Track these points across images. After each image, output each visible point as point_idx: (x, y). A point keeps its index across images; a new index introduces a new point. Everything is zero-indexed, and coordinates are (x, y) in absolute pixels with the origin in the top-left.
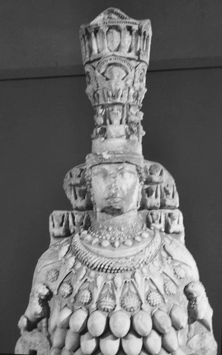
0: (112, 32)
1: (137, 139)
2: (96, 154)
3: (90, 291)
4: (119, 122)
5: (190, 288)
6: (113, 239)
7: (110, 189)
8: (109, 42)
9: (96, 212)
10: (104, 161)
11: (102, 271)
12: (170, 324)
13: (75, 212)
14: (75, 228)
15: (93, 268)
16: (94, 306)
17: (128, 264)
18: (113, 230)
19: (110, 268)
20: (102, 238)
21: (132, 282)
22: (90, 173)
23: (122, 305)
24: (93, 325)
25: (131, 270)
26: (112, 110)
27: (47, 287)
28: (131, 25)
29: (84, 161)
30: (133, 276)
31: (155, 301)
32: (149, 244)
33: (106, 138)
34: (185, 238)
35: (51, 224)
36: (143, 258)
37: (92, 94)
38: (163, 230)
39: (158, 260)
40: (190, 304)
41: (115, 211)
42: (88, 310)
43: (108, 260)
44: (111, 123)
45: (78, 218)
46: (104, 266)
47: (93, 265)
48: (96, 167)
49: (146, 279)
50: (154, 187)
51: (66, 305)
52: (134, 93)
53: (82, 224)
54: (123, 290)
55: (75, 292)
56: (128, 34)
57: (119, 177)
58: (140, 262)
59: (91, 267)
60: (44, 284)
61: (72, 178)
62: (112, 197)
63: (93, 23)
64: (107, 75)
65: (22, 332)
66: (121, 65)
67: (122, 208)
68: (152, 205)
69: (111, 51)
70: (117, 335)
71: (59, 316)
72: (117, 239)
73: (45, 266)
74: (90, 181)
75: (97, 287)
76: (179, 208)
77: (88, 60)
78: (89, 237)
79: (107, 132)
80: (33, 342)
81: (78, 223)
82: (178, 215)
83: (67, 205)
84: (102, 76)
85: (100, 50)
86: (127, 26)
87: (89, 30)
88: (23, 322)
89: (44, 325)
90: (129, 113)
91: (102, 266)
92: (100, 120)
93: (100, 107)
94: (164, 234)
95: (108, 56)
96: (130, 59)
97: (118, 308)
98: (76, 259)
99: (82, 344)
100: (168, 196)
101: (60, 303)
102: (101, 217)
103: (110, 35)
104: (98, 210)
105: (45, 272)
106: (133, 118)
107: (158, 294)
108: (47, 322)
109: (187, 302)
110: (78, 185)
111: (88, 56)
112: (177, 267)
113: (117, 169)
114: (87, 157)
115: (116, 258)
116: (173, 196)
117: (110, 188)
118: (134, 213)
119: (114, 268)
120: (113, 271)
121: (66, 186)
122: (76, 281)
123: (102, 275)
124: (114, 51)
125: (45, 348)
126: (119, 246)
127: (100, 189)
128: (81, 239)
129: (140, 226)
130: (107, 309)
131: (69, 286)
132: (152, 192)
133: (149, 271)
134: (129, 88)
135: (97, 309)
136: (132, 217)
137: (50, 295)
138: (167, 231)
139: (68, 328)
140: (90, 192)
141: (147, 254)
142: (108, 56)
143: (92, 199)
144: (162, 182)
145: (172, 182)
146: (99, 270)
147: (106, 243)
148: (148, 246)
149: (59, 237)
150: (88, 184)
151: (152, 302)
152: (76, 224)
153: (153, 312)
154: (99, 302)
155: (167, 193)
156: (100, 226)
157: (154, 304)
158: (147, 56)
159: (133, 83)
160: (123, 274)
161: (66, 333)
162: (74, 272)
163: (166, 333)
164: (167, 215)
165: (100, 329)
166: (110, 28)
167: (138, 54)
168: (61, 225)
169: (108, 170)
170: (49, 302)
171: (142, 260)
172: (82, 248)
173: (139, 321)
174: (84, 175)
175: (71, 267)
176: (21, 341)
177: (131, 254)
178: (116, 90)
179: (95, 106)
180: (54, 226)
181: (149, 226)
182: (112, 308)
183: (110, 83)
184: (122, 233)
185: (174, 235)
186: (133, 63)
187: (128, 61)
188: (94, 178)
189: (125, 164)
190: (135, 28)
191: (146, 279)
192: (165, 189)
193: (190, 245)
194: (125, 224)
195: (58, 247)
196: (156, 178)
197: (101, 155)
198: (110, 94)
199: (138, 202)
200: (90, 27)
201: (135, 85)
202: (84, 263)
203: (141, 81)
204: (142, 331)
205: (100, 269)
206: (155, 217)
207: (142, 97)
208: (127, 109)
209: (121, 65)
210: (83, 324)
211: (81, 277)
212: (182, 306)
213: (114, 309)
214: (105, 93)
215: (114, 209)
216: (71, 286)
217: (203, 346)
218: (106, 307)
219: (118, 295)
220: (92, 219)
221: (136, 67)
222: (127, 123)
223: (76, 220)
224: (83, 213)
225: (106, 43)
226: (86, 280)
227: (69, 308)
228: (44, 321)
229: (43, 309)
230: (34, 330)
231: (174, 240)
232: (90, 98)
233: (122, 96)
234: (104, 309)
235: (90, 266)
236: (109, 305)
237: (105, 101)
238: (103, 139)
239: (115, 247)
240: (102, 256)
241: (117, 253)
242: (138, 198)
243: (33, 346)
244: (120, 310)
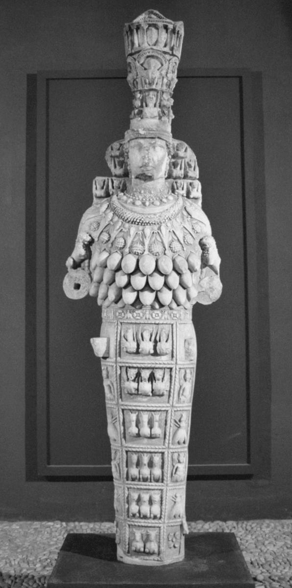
0: (151, 29)
1: (167, 120)
2: (133, 130)
3: (124, 239)
4: (153, 106)
5: (204, 241)
6: (144, 199)
7: (143, 159)
8: (148, 37)
9: (131, 178)
10: (140, 136)
11: (135, 224)
12: (187, 268)
13: (114, 178)
14: (114, 191)
15: (127, 221)
16: (127, 250)
17: (156, 219)
18: (145, 193)
19: (141, 222)
20: (135, 199)
21: (158, 232)
22: (128, 146)
23: (150, 251)
24: (126, 265)
25: (158, 224)
26: (148, 95)
27: (90, 236)
28: (167, 24)
29: (123, 137)
30: (159, 229)
31: (176, 248)
32: (173, 205)
33: (142, 118)
34: (203, 203)
35: (94, 187)
36: (168, 215)
37: (132, 81)
38: (185, 195)
39: (180, 218)
40: (203, 253)
41: (147, 178)
42: (122, 253)
43: (140, 215)
44: (147, 106)
45: (116, 183)
46: (137, 219)
47: (127, 219)
48: (133, 141)
49: (170, 231)
50: (179, 161)
51: (105, 249)
52: (168, 82)
53: (119, 188)
54: (151, 239)
55: (112, 239)
56: (164, 31)
57: (151, 150)
58: (166, 218)
59: (126, 220)
60: (87, 233)
61: (113, 150)
62: (145, 166)
63: (135, 21)
64: (146, 66)
65: (69, 269)
66: (157, 58)
67: (153, 175)
68: (178, 176)
69: (149, 45)
70: (145, 274)
71: (98, 257)
72: (148, 199)
73: (88, 219)
74: (127, 153)
75: (130, 235)
76: (199, 179)
77: (130, 52)
78: (125, 198)
79: (143, 113)
80: (78, 277)
81: (116, 187)
82: (198, 185)
83: (107, 173)
84: (141, 66)
85: (140, 44)
86: (164, 25)
87: (132, 26)
88: (70, 262)
90: (162, 98)
91: (135, 220)
92: (137, 103)
93: (138, 92)
94: (186, 198)
95: (146, 50)
96: (165, 53)
97: (146, 252)
98: (113, 214)
99: (117, 279)
100: (190, 169)
102: (135, 183)
103: (149, 32)
104: (133, 177)
105: (88, 224)
106: (165, 103)
107: (178, 243)
108: (89, 263)
109: (201, 251)
110: (117, 157)
111: (130, 49)
112: (194, 224)
113: (150, 143)
114: (126, 133)
115: (146, 214)
116: (194, 170)
117: (144, 158)
118: (162, 181)
119: (144, 222)
120: (143, 224)
121: (107, 158)
122: (114, 230)
124: (153, 45)
125: (87, 282)
126: (149, 205)
127: (135, 159)
128: (118, 199)
129: (166, 191)
130: (138, 253)
131: (107, 235)
132: (178, 164)
133: (172, 225)
134: (163, 78)
135: (130, 253)
136: (160, 183)
137: (92, 242)
138: (188, 196)
139: (106, 267)
140: (127, 163)
141: (172, 212)
142: (146, 50)
143: (128, 168)
144: (186, 157)
145: (195, 158)
146: (132, 223)
147: (138, 203)
148: (172, 206)
149: (100, 197)
150: (126, 156)
151: (174, 249)
152: (115, 187)
153: (174, 257)
154: (131, 247)
155: (190, 166)
156: (134, 190)
157: (175, 251)
158: (179, 51)
159: (167, 73)
160: (152, 226)
161: (104, 271)
162: (112, 223)
163: (183, 273)
164: (189, 183)
165: (132, 268)
166: (150, 25)
167: (172, 49)
168: (102, 188)
169: (143, 144)
170: (91, 247)
171: (167, 216)
172: (119, 206)
173: (162, 263)
174: (123, 148)
175: (109, 220)
176: (68, 276)
177: (159, 212)
178: (152, 78)
179: (134, 92)
180: (96, 188)
181: (173, 191)
182: (142, 252)
183: (147, 72)
184: (152, 195)
185: (194, 200)
186: (168, 57)
187: (163, 54)
188: (131, 150)
189: (157, 139)
190: (171, 27)
191: (170, 231)
192: (188, 163)
193: (205, 208)
194: (155, 189)
195: (99, 205)
196: (181, 153)
197: (138, 131)
198: (147, 81)
199: (166, 172)
200: (133, 24)
201: (168, 75)
203: (173, 72)
204: (164, 270)
205: (133, 222)
206: (179, 185)
207: (173, 86)
208: (161, 95)
209: (157, 58)
210: (118, 264)
211: (118, 227)
212: (197, 254)
213: (143, 253)
214: (143, 81)
215: (146, 176)
216: (109, 235)
217: (211, 286)
218: (137, 251)
219: (147, 242)
220: (128, 185)
221: (170, 60)
222: (160, 106)
223: (114, 185)
224: (121, 179)
225: (145, 39)
226: (122, 230)
227: (108, 252)
228: (87, 261)
229: (86, 252)
230: (78, 269)
231: (193, 203)
232: (130, 85)
233: (157, 84)
234: (135, 252)
235: (125, 220)
236: (139, 250)
237: (143, 87)
238: (140, 119)
239: (146, 206)
240: (135, 212)
241: (147, 210)
242: (166, 168)
243: (77, 280)
244: (148, 254)
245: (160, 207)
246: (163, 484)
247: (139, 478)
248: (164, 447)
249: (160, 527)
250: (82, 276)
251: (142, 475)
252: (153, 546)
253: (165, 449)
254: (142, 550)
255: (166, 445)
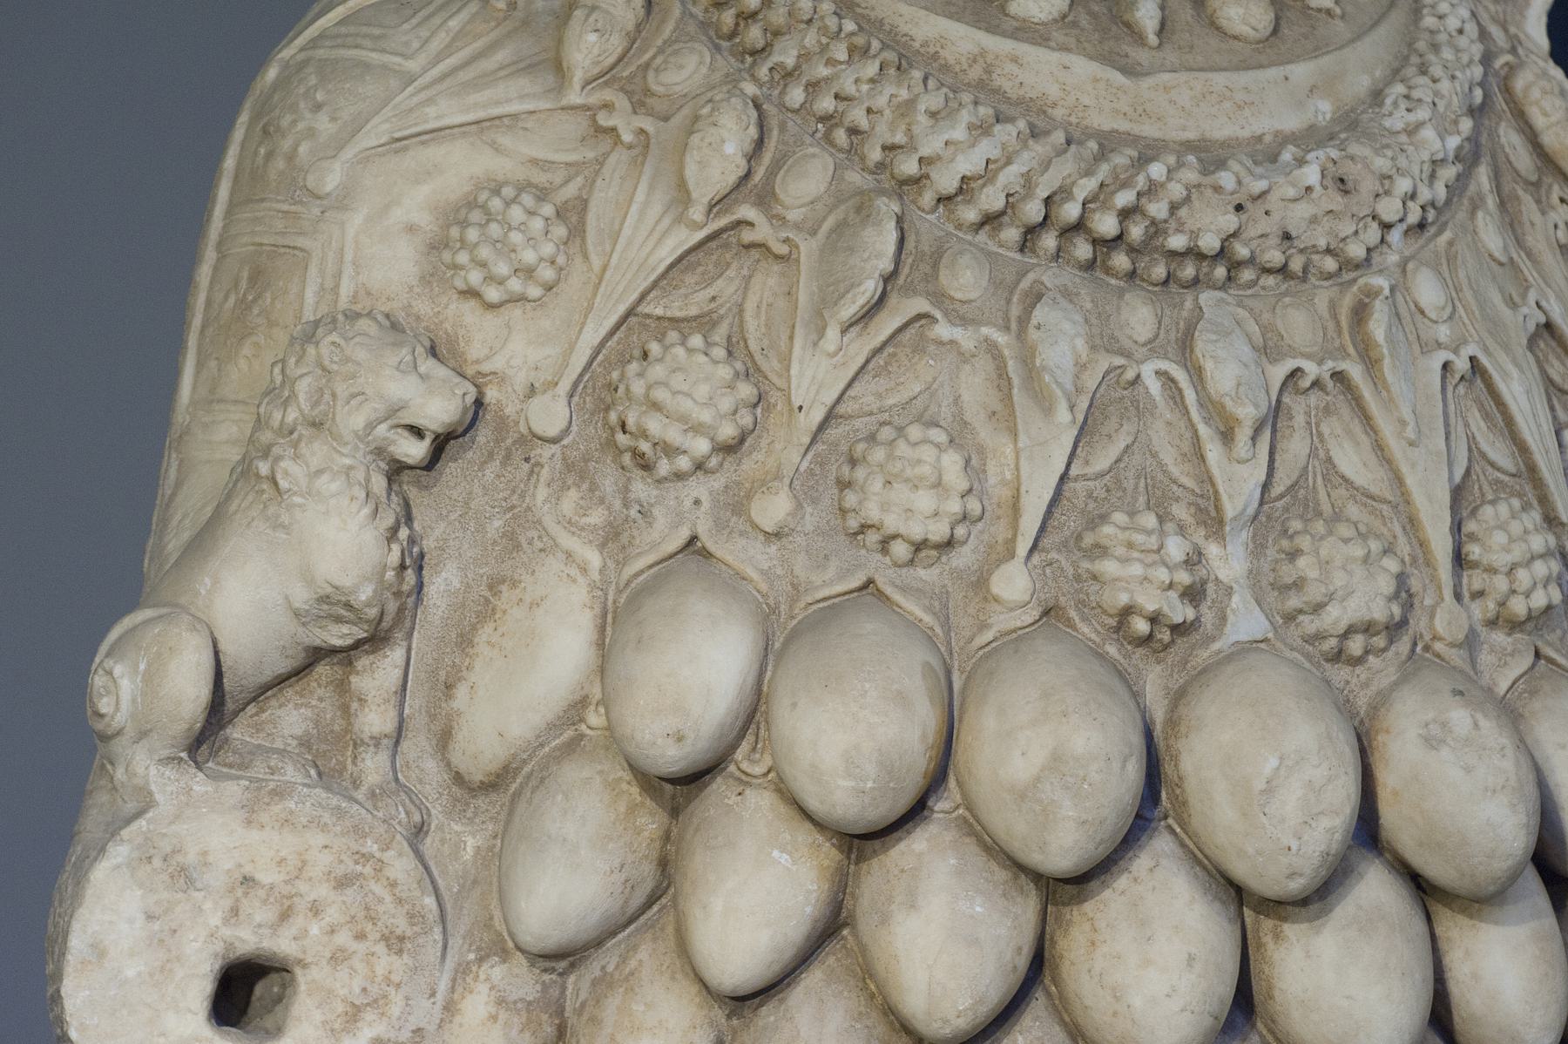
80: (265, 878)
89: (375, 720)
91: (1071, 211)
101: (596, 517)
119: (1177, 242)
123: (1067, 294)
125: (395, 943)
171: (1403, 185)
202: (875, 155)
228: (378, 676)
234: (1127, 611)
241: (1183, 103)
245: (1302, 71)
250: (321, 861)
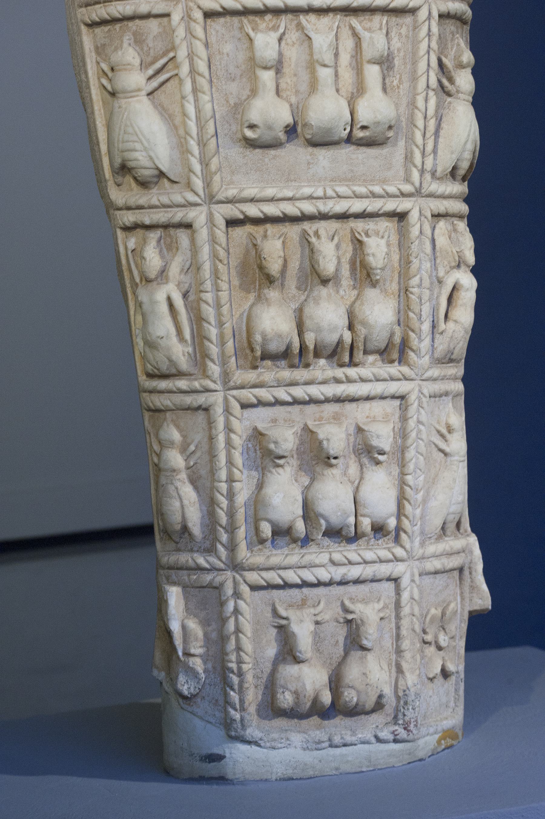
246: (405, 369)
247: (303, 348)
248: (407, 188)
249: (396, 580)
251: (318, 330)
252: (371, 674)
253: (409, 195)
254: (327, 698)
255: (416, 175)
